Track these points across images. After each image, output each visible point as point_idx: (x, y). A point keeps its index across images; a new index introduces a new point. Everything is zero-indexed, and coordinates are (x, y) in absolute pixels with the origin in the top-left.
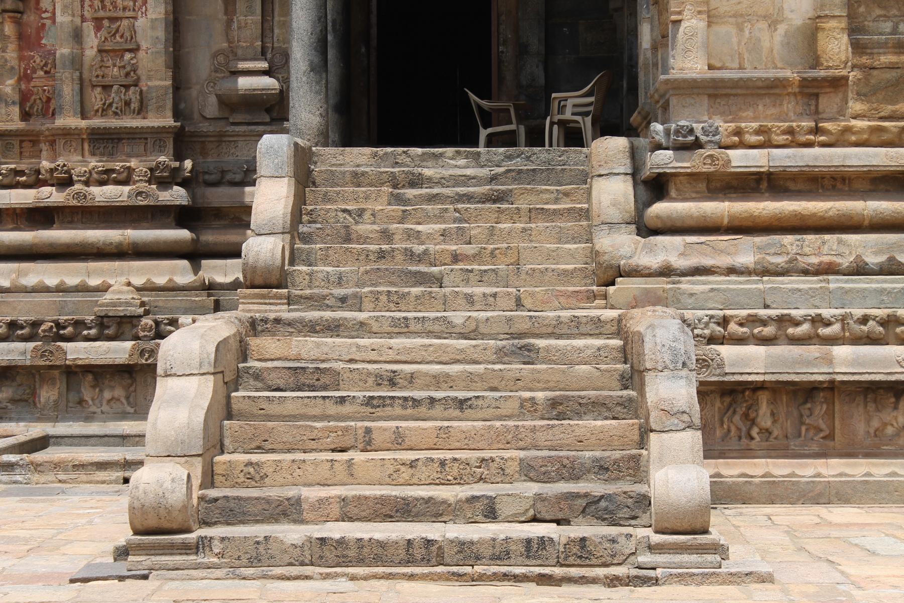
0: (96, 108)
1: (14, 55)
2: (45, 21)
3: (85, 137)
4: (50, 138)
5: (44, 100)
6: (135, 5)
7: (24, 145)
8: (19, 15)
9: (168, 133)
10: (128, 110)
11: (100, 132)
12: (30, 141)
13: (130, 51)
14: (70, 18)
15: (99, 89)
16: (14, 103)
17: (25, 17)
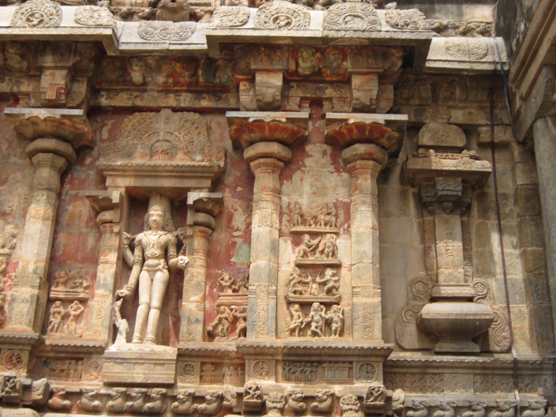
0: (292, 326)
1: (202, 271)
2: (236, 239)
3: (280, 358)
4: (236, 361)
5: (230, 320)
6: (336, 221)
7: (205, 367)
8: (210, 231)
9: (377, 356)
10: (328, 330)
11: (299, 352)
12: (213, 364)
13: (332, 266)
14: (268, 229)
15: (297, 306)
16: (197, 321)
17: (215, 234)
